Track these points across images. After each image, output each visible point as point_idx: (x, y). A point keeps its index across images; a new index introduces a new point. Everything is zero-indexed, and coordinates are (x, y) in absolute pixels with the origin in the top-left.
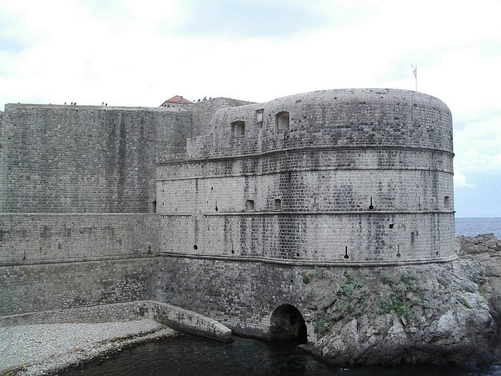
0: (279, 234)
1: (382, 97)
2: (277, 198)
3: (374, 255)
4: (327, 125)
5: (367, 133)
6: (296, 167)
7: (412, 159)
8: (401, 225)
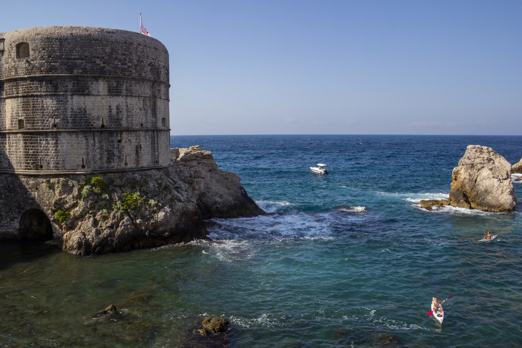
0: (24, 149)
1: (112, 36)
2: (20, 118)
3: (105, 165)
4: (64, 57)
5: (99, 65)
6: (37, 92)
8: (127, 140)
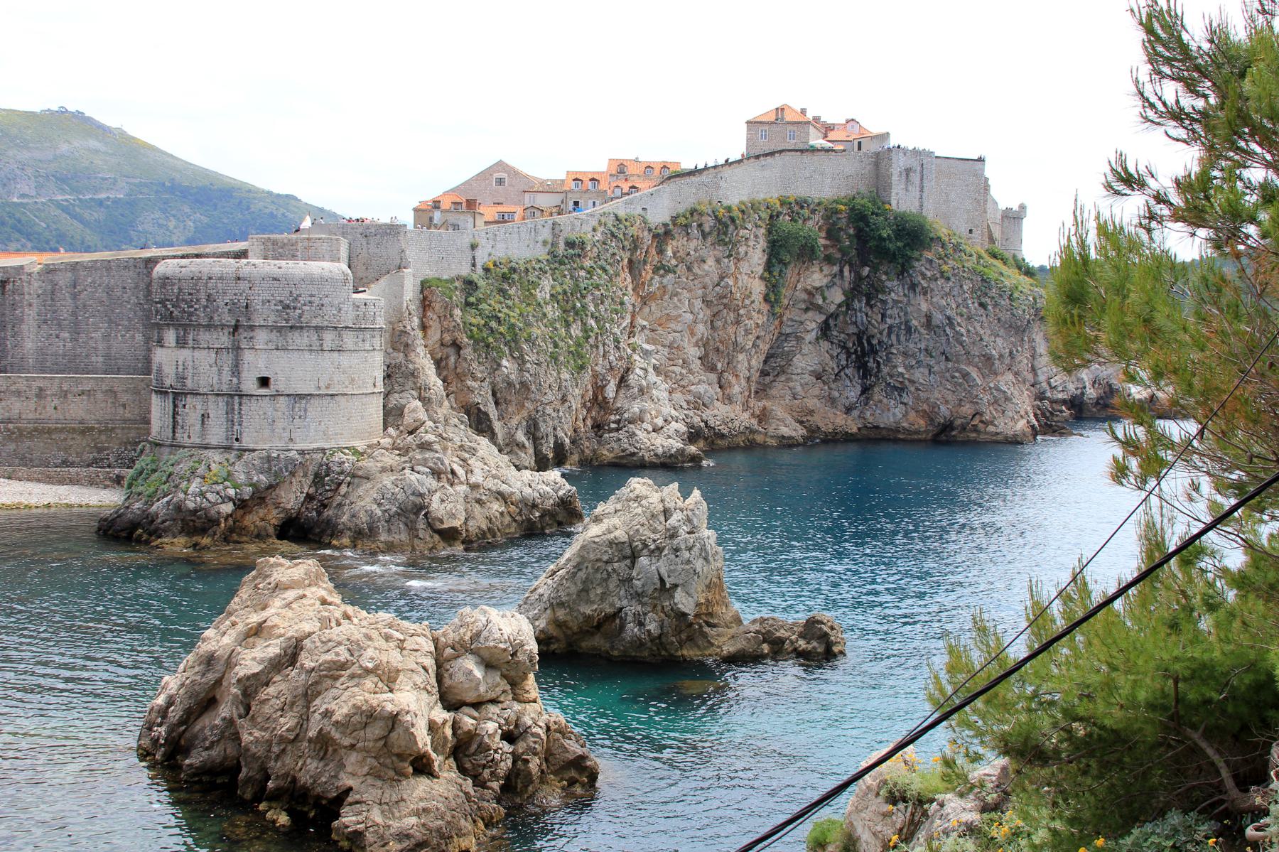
7: (204, 336)
